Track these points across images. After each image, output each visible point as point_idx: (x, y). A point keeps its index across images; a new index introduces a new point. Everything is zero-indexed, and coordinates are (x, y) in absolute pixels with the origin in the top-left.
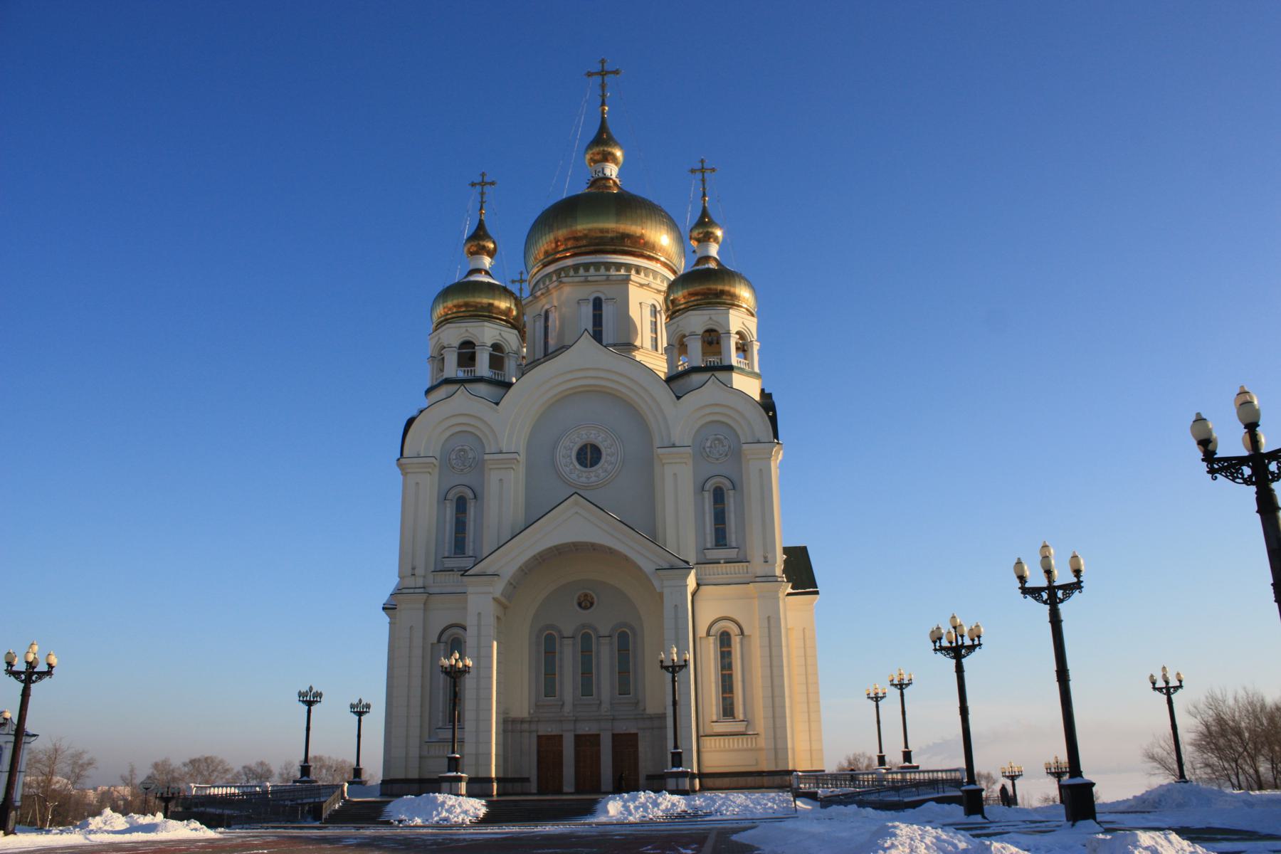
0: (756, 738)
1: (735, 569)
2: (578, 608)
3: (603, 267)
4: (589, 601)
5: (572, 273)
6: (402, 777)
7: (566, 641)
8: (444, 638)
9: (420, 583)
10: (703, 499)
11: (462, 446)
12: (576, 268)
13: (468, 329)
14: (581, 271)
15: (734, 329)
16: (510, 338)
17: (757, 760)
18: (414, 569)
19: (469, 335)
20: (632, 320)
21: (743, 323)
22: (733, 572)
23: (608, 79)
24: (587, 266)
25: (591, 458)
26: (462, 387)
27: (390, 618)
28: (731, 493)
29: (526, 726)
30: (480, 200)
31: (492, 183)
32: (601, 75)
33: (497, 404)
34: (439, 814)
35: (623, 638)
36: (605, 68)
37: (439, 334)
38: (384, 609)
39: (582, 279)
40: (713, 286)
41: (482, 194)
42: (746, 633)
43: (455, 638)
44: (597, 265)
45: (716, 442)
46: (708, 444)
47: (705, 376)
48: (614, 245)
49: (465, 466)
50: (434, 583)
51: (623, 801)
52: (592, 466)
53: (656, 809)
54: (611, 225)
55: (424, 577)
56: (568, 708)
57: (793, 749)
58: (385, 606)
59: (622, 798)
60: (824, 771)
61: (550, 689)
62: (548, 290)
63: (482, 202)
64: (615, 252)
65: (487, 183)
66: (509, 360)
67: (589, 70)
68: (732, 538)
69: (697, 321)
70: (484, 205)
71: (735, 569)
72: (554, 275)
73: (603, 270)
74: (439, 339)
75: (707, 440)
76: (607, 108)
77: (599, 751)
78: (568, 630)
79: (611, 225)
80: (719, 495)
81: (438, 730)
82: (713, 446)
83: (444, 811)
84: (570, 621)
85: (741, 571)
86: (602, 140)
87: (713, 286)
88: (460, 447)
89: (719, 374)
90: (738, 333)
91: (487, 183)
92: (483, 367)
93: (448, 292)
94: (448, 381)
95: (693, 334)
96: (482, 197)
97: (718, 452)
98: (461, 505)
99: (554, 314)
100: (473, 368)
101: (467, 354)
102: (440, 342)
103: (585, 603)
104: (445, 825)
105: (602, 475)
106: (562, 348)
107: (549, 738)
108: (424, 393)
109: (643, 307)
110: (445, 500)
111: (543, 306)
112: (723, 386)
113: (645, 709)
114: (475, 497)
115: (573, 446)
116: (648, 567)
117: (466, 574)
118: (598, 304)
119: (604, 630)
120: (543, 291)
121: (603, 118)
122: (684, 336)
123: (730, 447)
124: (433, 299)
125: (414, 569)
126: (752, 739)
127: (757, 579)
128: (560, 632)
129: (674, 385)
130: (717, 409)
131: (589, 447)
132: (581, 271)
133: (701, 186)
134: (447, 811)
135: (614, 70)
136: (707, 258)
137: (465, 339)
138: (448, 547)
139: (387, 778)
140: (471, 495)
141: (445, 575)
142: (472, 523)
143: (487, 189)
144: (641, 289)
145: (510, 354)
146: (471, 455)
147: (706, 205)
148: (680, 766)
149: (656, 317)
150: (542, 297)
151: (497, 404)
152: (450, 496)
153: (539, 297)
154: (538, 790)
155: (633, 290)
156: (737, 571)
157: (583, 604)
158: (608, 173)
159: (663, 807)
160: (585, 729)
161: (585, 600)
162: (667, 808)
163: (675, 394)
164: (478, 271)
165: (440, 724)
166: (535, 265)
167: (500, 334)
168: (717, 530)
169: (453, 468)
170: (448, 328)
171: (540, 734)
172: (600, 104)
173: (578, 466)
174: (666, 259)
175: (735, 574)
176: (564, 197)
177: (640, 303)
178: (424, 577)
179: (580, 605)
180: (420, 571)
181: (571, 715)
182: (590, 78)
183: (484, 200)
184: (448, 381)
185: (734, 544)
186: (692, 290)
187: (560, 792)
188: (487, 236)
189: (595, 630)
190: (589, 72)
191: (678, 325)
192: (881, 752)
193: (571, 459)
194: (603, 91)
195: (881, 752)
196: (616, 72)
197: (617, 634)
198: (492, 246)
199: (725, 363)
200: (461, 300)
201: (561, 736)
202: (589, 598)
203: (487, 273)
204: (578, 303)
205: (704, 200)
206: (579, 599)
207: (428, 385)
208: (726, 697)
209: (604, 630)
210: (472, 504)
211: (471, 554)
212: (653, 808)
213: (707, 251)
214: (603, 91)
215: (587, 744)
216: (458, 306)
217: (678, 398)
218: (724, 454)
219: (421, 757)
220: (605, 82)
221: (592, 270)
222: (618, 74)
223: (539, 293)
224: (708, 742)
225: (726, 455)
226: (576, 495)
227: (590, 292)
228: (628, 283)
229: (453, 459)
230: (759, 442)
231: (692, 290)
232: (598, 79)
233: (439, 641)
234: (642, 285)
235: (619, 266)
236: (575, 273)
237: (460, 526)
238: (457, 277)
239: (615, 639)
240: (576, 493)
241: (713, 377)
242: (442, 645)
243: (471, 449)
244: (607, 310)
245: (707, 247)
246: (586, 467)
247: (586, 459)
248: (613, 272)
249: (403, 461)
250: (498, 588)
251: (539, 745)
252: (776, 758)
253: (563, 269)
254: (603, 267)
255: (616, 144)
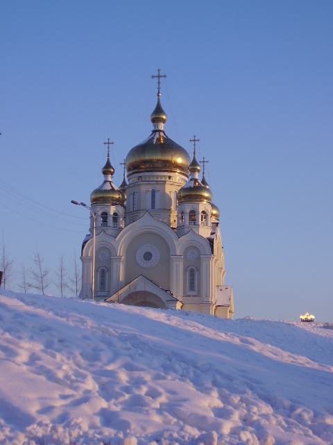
15: (201, 211)
16: (121, 210)
54: (158, 157)
64: (160, 171)
69: (188, 208)
79: (158, 157)
90: (203, 212)
116: (164, 300)
118: (153, 192)
155: (167, 186)
198: (112, 170)
232: (156, 79)
235: (161, 177)
244: (157, 195)
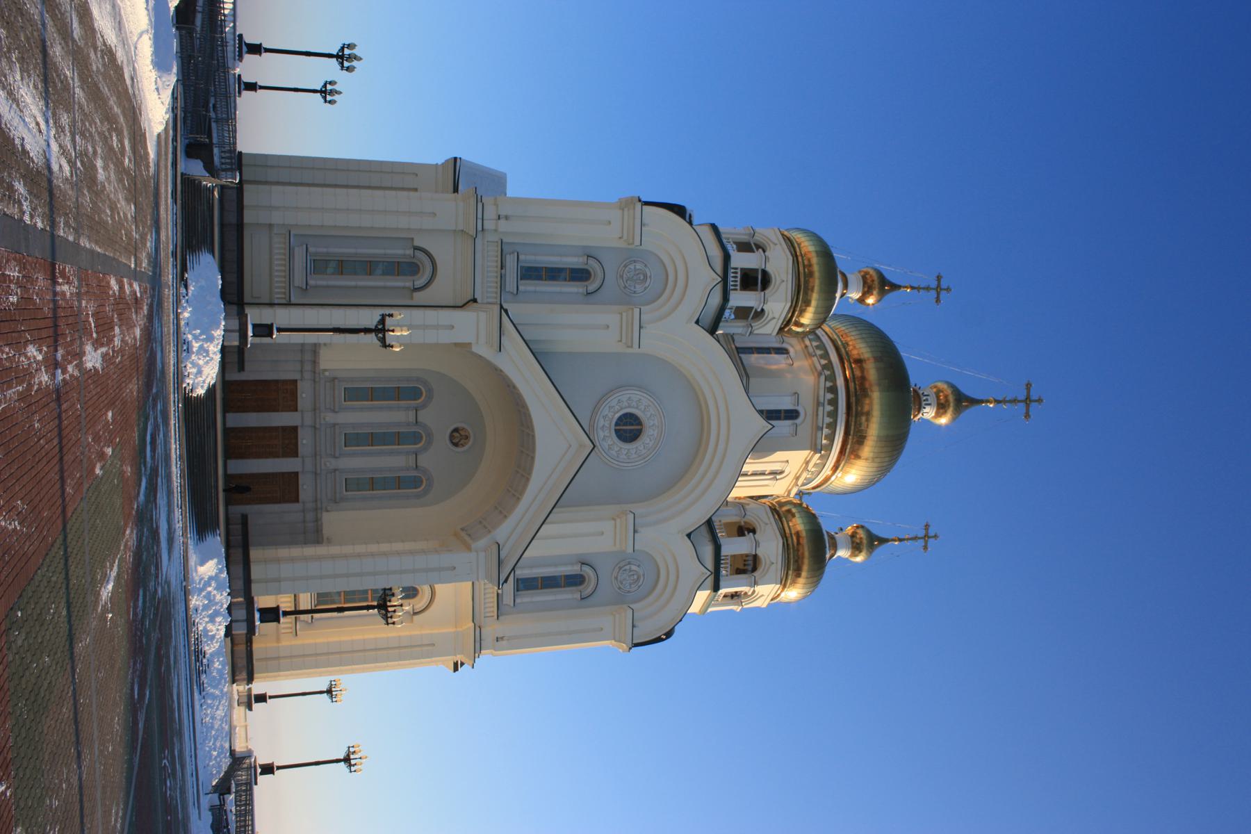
0: (291, 632)
1: (491, 602)
2: (452, 428)
3: (831, 420)
4: (459, 441)
5: (829, 384)
6: (246, 202)
7: (412, 414)
8: (418, 253)
9: (489, 225)
10: (572, 564)
11: (650, 277)
12: (833, 390)
13: (784, 284)
14: (829, 396)
15: (758, 588)
16: (767, 330)
17: (266, 635)
18: (507, 218)
19: (777, 283)
20: (770, 455)
21: (762, 595)
22: (487, 591)
23: (1022, 407)
24: (834, 402)
25: (625, 431)
26: (720, 279)
27: (443, 164)
28: (578, 596)
29: (308, 367)
30: (921, 286)
31: (938, 300)
32: (1027, 399)
33: (697, 322)
34: (196, 338)
35: (415, 482)
36: (1033, 404)
37: (781, 244)
38: (455, 159)
39: (821, 400)
40: (806, 561)
41: (928, 288)
42: (416, 617)
43: (419, 270)
44: (833, 414)
45: (635, 577)
46: (634, 568)
47: (710, 563)
48: (854, 434)
49: (627, 281)
50: (488, 242)
51: (216, 575)
52: (616, 431)
53: (207, 619)
54: (874, 429)
55: (496, 230)
56: (330, 418)
57: (279, 676)
58: (458, 161)
59: (221, 571)
60: (256, 784)
61: (355, 394)
62: (811, 355)
63: (918, 288)
64: (847, 433)
65: (938, 294)
66: (743, 327)
67: (1033, 385)
68: (527, 598)
69: (770, 547)
70: (916, 291)
71: (490, 607)
72: (826, 362)
73: (828, 420)
74: (776, 244)
75: (639, 566)
76: (991, 406)
77: (277, 456)
78: (426, 416)
79: (874, 429)
80: (575, 581)
81: (305, 246)
82: (632, 573)
83: (201, 343)
84: (437, 419)
85: (487, 610)
86: (961, 401)
87: (806, 561)
88: (649, 274)
89: (710, 581)
91: (938, 294)
92: (740, 299)
93: (826, 255)
94: (727, 258)
95: (757, 544)
96: (923, 288)
97: (625, 579)
98: (580, 275)
99: (783, 362)
100: (738, 287)
101: (755, 280)
102: (772, 245)
103: (457, 437)
104: (183, 347)
105: (605, 445)
106: (745, 374)
107: (294, 394)
108: (712, 222)
109: (784, 464)
110: (588, 256)
111: (792, 346)
112: (698, 585)
113: (328, 511)
114: (588, 294)
115: (640, 410)
116: (502, 532)
117: (502, 311)
118: (792, 415)
119: (425, 460)
120: (811, 350)
121: (982, 401)
122: (754, 531)
123: (629, 592)
124: (815, 232)
125: (507, 218)
126: (291, 628)
127: (478, 628)
128: (424, 406)
129: (704, 530)
130: (672, 578)
131: (639, 427)
132: (829, 396)
133: (911, 537)
134: (201, 347)
135: (1030, 413)
136: (835, 547)
137: (773, 276)
138: (530, 259)
139: (244, 161)
140: (591, 288)
141: (497, 261)
142: (557, 289)
143: (933, 294)
144: (803, 460)
145: (750, 329)
146: (639, 288)
147: (890, 543)
148: (262, 621)
149: (770, 474)
150: (803, 346)
151: (697, 322)
152: (591, 261)
153: (803, 341)
154: (228, 381)
155: (804, 454)
156: (487, 600)
157: (456, 434)
158: (927, 409)
159: (210, 626)
160: (305, 441)
161: (461, 435)
162: (208, 631)
163: (693, 531)
164: (846, 286)
165: (311, 249)
166: (831, 328)
167: (774, 318)
168: (534, 579)
169: (625, 266)
170: (788, 259)
171: (299, 384)
172: (997, 398)
173: (617, 415)
174: (832, 482)
175: (485, 603)
176: (902, 354)
177: (787, 461)
178: (496, 230)
179: (456, 430)
180: (503, 226)
181: (323, 422)
182: (1025, 387)
183: (921, 291)
184: (727, 258)
185: (518, 601)
186: (804, 541)
187: (227, 456)
188: (882, 293)
189: (425, 449)
190: (1031, 385)
191: (767, 524)
192: (271, 697)
193: (626, 408)
194: (1010, 401)
195: (271, 697)
196: (1027, 415)
197: (420, 475)
199: (722, 583)
200: (816, 268)
201: (296, 410)
202: (462, 442)
203: (843, 295)
204: (796, 393)
205: (895, 540)
206: (463, 429)
207: (721, 229)
208: (340, 596)
209: (424, 460)
210: (581, 290)
211: (521, 288)
212: (208, 616)
213: (842, 548)
214: (1010, 401)
215: (287, 441)
216: (810, 265)
217: (689, 536)
218: (621, 586)
219: (271, 226)
220: (1018, 404)
221: (829, 408)
222: (1026, 417)
223: (807, 342)
224: (288, 599)
225: (620, 588)
226: (592, 446)
227: (806, 407)
228: (811, 449)
229: (635, 266)
230: (633, 626)
231: (804, 541)
233: (416, 248)
234: (807, 463)
235: (831, 438)
236: (828, 388)
237: (553, 274)
238: (841, 265)
239: (414, 473)
240: (594, 446)
241: (709, 573)
242: (410, 252)
243: (645, 289)
245: (847, 548)
246: (617, 424)
247: (625, 424)
248: (826, 431)
249: (639, 205)
250: (484, 350)
251: (285, 382)
252: (267, 659)
253: (834, 372)
254: (831, 420)
255: (954, 419)
